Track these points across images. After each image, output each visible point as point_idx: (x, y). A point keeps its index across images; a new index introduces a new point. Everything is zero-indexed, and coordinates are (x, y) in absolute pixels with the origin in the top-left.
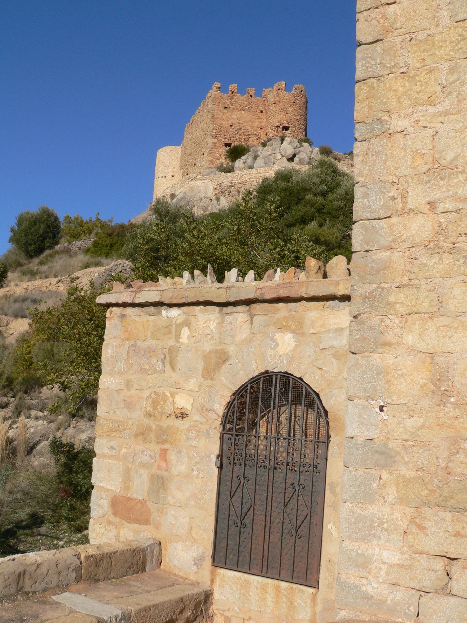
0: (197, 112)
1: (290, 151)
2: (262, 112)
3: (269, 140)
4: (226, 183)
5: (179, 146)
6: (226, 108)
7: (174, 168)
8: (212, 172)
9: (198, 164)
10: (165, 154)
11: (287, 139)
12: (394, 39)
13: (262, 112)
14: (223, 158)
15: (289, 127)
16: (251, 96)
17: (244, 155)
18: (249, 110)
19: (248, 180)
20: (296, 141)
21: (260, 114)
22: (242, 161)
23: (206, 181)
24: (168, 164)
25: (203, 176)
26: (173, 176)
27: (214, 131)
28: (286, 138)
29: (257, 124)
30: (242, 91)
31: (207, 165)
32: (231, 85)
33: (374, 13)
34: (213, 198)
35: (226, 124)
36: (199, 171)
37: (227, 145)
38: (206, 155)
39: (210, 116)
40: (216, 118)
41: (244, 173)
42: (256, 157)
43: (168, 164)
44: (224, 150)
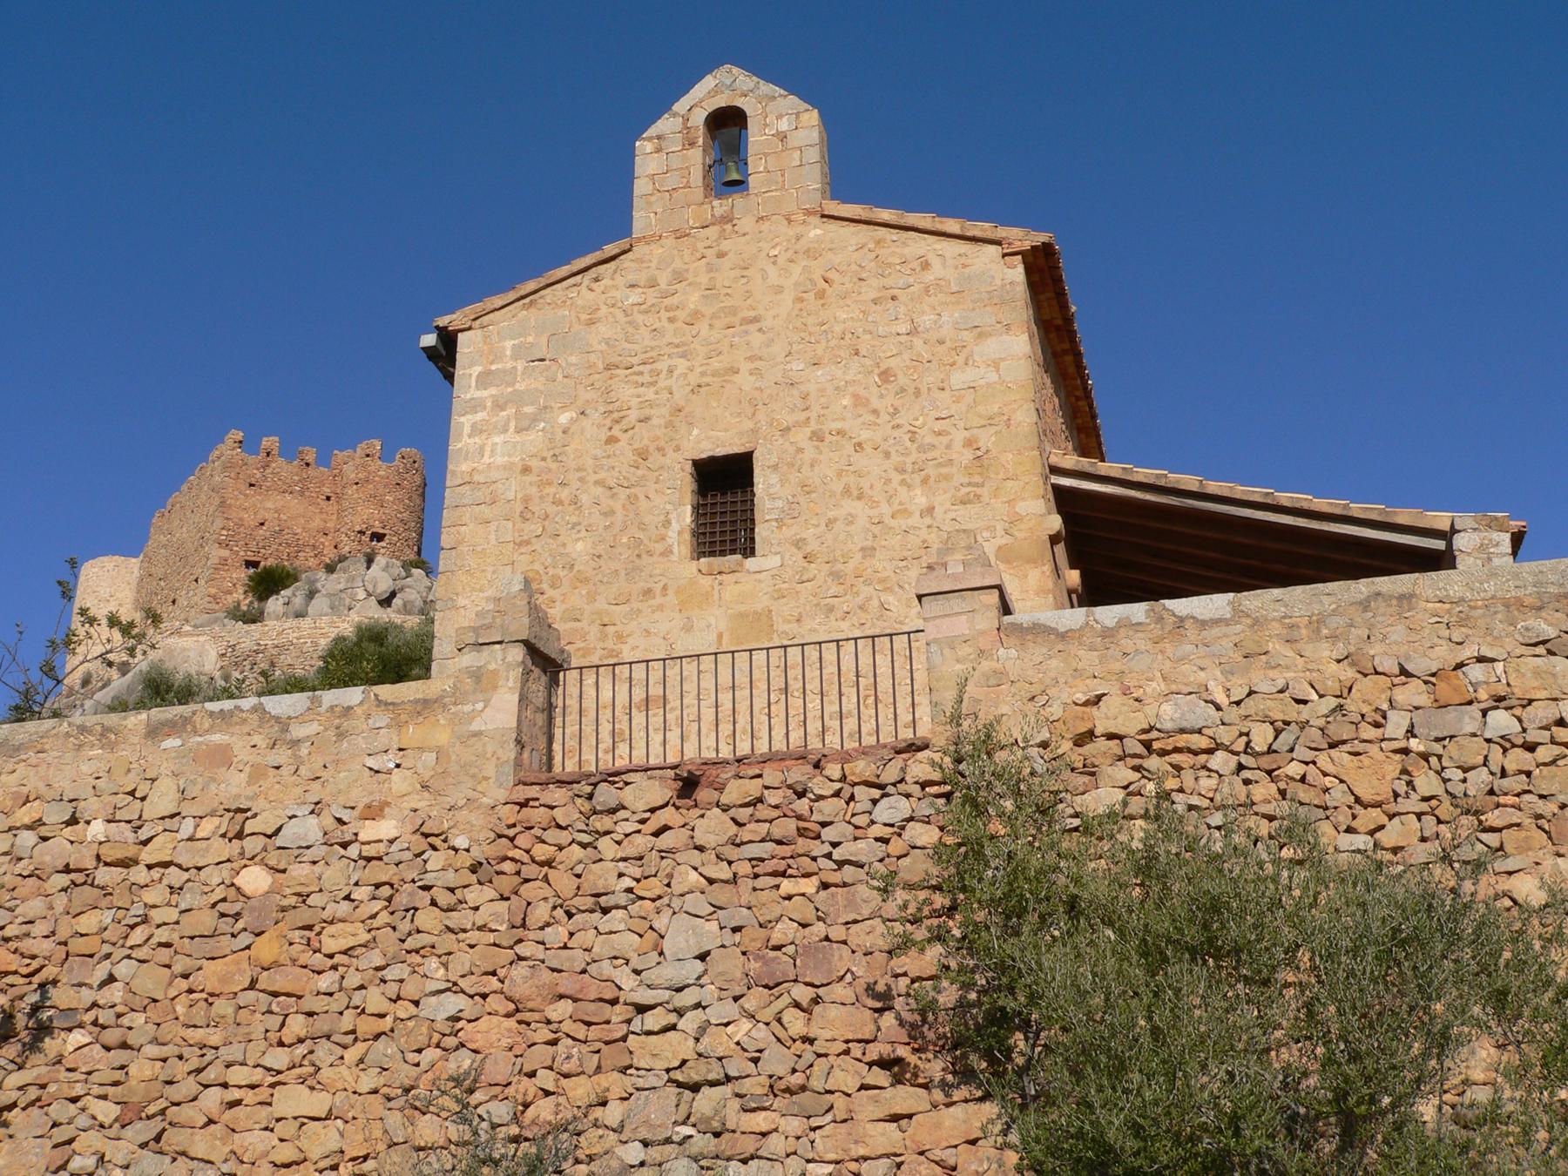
0: (184, 487)
1: (384, 586)
3: (342, 559)
4: (247, 644)
8: (216, 620)
9: (182, 602)
11: (380, 560)
12: (464, 548)
13: (328, 498)
14: (241, 591)
17: (286, 587)
18: (302, 493)
20: (399, 563)
21: (324, 504)
22: (281, 601)
23: (201, 639)
25: (195, 626)
28: (378, 558)
29: (317, 523)
30: (288, 453)
31: (204, 603)
33: (453, 530)
35: (250, 519)
36: (183, 616)
37: (250, 564)
38: (202, 582)
39: (217, 501)
42: (311, 594)
44: (243, 574)
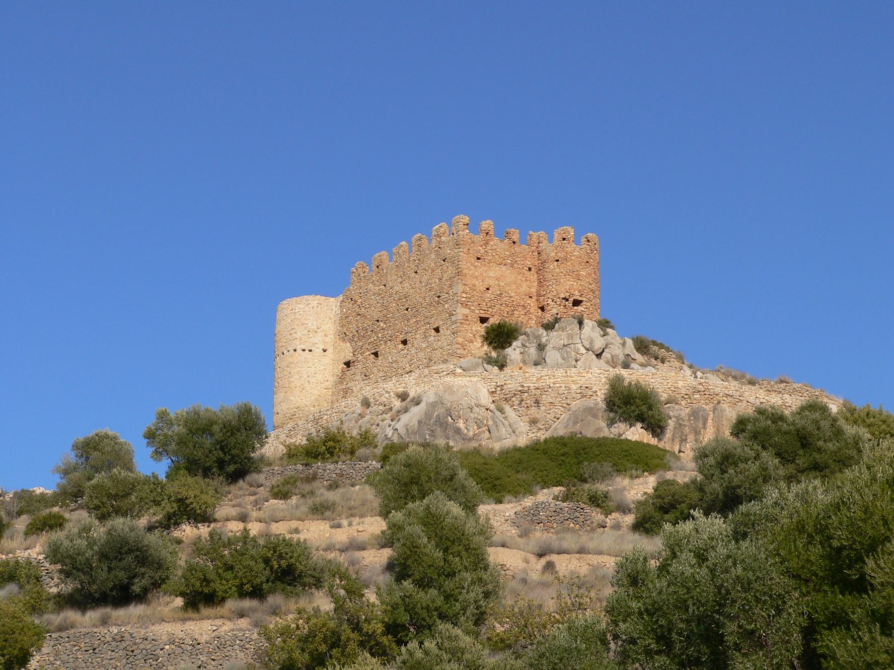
2: (530, 269)
3: (557, 320)
4: (512, 386)
5: (334, 295)
6: (479, 259)
7: (326, 335)
10: (307, 309)
13: (530, 269)
14: (479, 340)
15: (581, 301)
16: (514, 243)
17: (516, 339)
19: (552, 385)
21: (527, 273)
22: (518, 351)
23: (474, 379)
24: (314, 327)
26: (325, 351)
27: (464, 295)
28: (586, 321)
29: (524, 288)
32: (484, 222)
34: (492, 407)
37: (483, 320)
40: (465, 275)
41: (544, 373)
42: (541, 347)
43: (314, 327)
44: (481, 329)
